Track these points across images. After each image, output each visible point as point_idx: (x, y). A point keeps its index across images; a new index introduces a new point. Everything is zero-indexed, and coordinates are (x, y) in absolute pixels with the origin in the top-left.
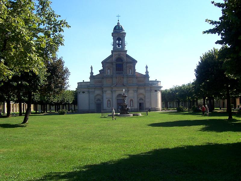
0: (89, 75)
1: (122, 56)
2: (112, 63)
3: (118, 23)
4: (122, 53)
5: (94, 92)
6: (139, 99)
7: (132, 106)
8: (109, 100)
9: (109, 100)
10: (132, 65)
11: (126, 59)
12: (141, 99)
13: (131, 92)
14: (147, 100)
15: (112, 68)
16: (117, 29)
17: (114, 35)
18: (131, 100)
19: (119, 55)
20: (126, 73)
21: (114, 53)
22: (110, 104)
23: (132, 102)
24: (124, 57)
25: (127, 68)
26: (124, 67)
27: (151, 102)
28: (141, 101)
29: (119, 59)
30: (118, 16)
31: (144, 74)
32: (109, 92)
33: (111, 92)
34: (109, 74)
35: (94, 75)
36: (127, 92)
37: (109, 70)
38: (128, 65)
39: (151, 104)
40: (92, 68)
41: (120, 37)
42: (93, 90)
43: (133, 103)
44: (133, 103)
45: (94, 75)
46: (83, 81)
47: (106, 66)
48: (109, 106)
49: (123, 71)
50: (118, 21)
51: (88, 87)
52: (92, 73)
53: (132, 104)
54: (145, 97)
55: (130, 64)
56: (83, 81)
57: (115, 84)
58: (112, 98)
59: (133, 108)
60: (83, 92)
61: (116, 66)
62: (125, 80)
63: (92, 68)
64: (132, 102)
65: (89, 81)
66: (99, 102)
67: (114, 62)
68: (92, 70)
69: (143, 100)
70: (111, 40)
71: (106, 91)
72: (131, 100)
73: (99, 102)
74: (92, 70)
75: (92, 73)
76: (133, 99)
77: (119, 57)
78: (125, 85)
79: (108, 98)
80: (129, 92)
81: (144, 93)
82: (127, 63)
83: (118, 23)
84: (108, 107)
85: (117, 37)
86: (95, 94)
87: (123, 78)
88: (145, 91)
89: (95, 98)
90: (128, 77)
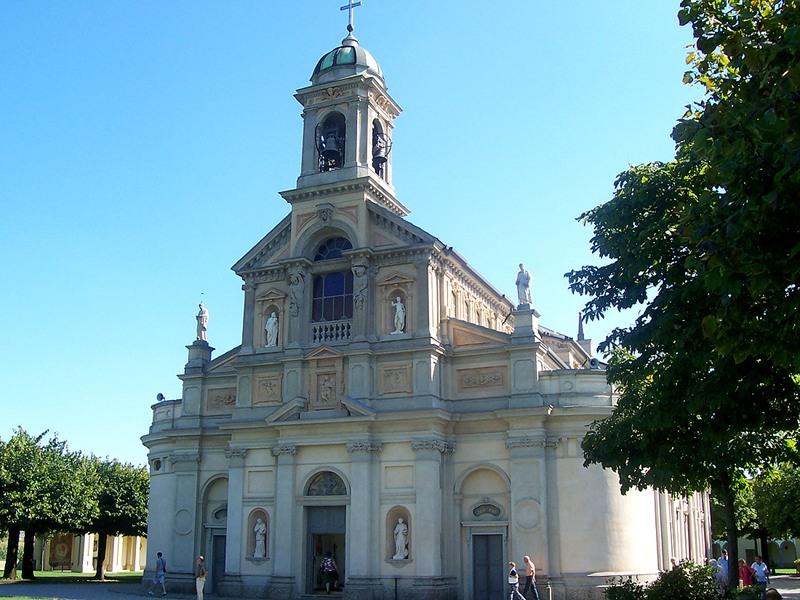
0: (182, 359)
1: (341, 218)
2: (282, 270)
4: (341, 201)
6: (470, 504)
7: (399, 556)
9: (259, 515)
10: (407, 270)
12: (487, 508)
13: (397, 453)
15: (287, 307)
18: (400, 516)
20: (371, 327)
23: (401, 528)
24: (348, 221)
25: (378, 296)
26: (360, 283)
28: (487, 525)
29: (331, 244)
32: (260, 458)
33: (270, 460)
34: (272, 340)
36: (365, 455)
37: (272, 321)
38: (384, 273)
41: (337, 109)
42: (192, 449)
43: (407, 534)
44: (407, 534)
46: (160, 396)
48: (259, 554)
49: (350, 315)
50: (350, 28)
51: (174, 429)
52: (201, 347)
53: (400, 541)
55: (397, 268)
56: (160, 396)
58: (272, 500)
59: (406, 571)
61: (316, 292)
62: (358, 374)
64: (401, 528)
65: (181, 398)
67: (292, 264)
68: (201, 328)
71: (244, 454)
72: (400, 516)
74: (201, 328)
75: (201, 347)
76: (410, 507)
78: (351, 406)
79: (252, 500)
80: (384, 457)
81: (503, 466)
82: (374, 259)
84: (251, 558)
85: (321, 115)
86: (206, 476)
87: (345, 359)
90: (378, 352)
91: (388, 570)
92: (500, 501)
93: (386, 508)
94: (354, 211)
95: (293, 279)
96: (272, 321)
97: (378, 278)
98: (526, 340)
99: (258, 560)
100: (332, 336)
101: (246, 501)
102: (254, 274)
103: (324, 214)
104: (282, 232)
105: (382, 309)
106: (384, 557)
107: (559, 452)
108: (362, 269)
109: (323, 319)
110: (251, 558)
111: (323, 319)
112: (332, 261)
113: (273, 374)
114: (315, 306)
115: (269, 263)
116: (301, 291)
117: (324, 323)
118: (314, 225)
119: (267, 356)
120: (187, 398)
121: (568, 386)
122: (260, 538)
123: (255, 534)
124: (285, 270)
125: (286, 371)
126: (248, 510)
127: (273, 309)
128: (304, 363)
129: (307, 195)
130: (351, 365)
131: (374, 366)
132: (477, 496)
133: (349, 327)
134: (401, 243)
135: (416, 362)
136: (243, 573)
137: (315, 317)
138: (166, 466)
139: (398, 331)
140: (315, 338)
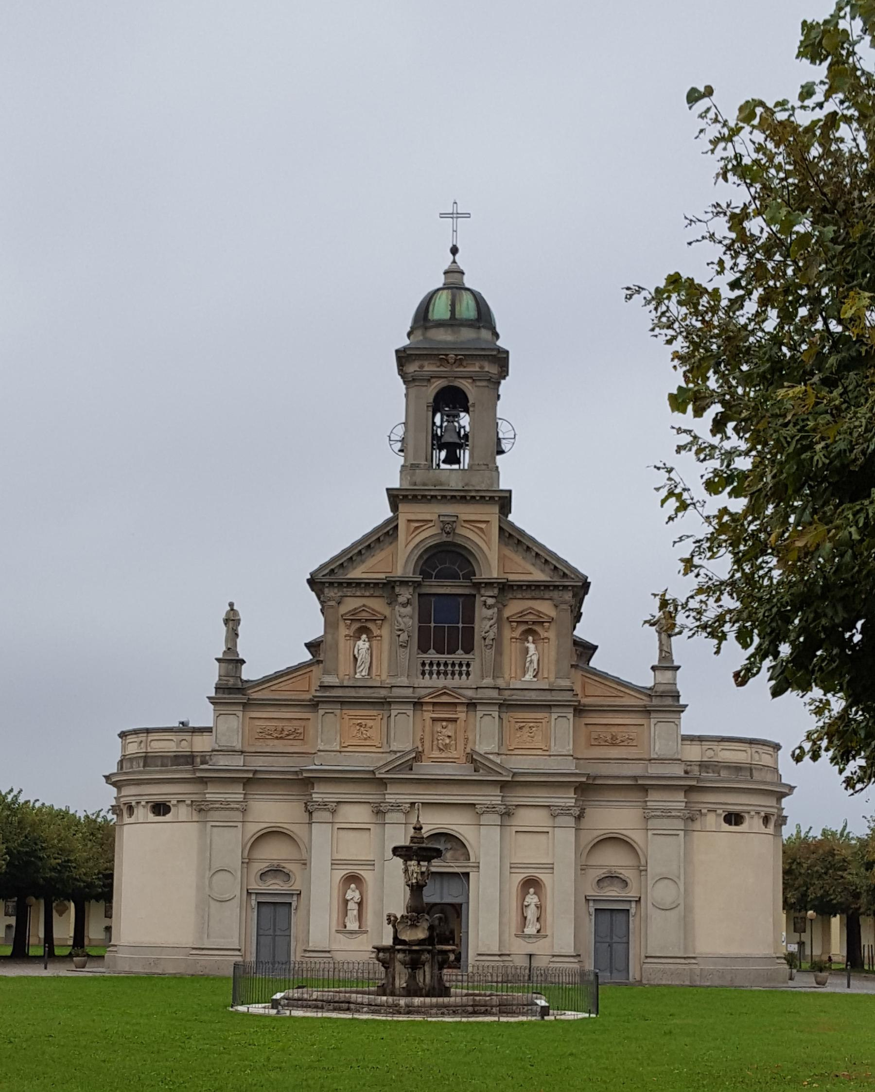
0: (212, 675)
2: (388, 587)
3: (454, 273)
4: (466, 512)
5: (244, 811)
7: (531, 930)
8: (353, 879)
11: (502, 558)
14: (662, 893)
16: (440, 324)
17: (412, 368)
19: (448, 526)
21: (407, 512)
22: (360, 904)
27: (688, 910)
29: (447, 557)
30: (455, 215)
31: (646, 679)
34: (362, 672)
35: (248, 673)
36: (496, 819)
38: (514, 607)
39: (687, 925)
40: (232, 620)
45: (248, 673)
47: (343, 609)
48: (353, 925)
50: (454, 250)
52: (232, 661)
53: (531, 913)
54: (641, 870)
57: (395, 752)
59: (538, 947)
60: (160, 808)
61: (423, 617)
63: (232, 620)
66: (275, 885)
67: (404, 583)
68: (233, 635)
69: (625, 883)
70: (389, 401)
73: (275, 885)
74: (233, 635)
75: (232, 661)
77: (445, 538)
82: (506, 588)
83: (454, 273)
85: (437, 385)
86: (253, 829)
88: (646, 819)
89: (247, 862)
91: (519, 948)
92: (626, 874)
93: (518, 878)
94: (483, 526)
95: (401, 599)
96: (362, 645)
97: (507, 613)
98: (669, 701)
99: (352, 932)
100: (446, 674)
101: (335, 863)
102: (340, 584)
103: (448, 526)
104: (386, 534)
105: (511, 650)
106: (514, 932)
107: (697, 826)
108: (490, 601)
109: (432, 651)
110: (343, 929)
111: (432, 651)
112: (448, 582)
113: (375, 713)
114: (423, 632)
115: (357, 573)
116: (405, 616)
117: (432, 655)
118: (429, 534)
119: (362, 693)
120: (222, 727)
121: (710, 753)
122: (352, 906)
123: (346, 902)
124: (393, 587)
125: (394, 713)
126: (340, 874)
127: (363, 630)
128: (418, 704)
129: (424, 496)
130: (479, 714)
131: (504, 715)
132: (601, 867)
133: (468, 665)
134: (539, 575)
135: (554, 716)
136: (334, 947)
137: (423, 648)
138: (181, 812)
139: (529, 677)
140: (423, 673)
